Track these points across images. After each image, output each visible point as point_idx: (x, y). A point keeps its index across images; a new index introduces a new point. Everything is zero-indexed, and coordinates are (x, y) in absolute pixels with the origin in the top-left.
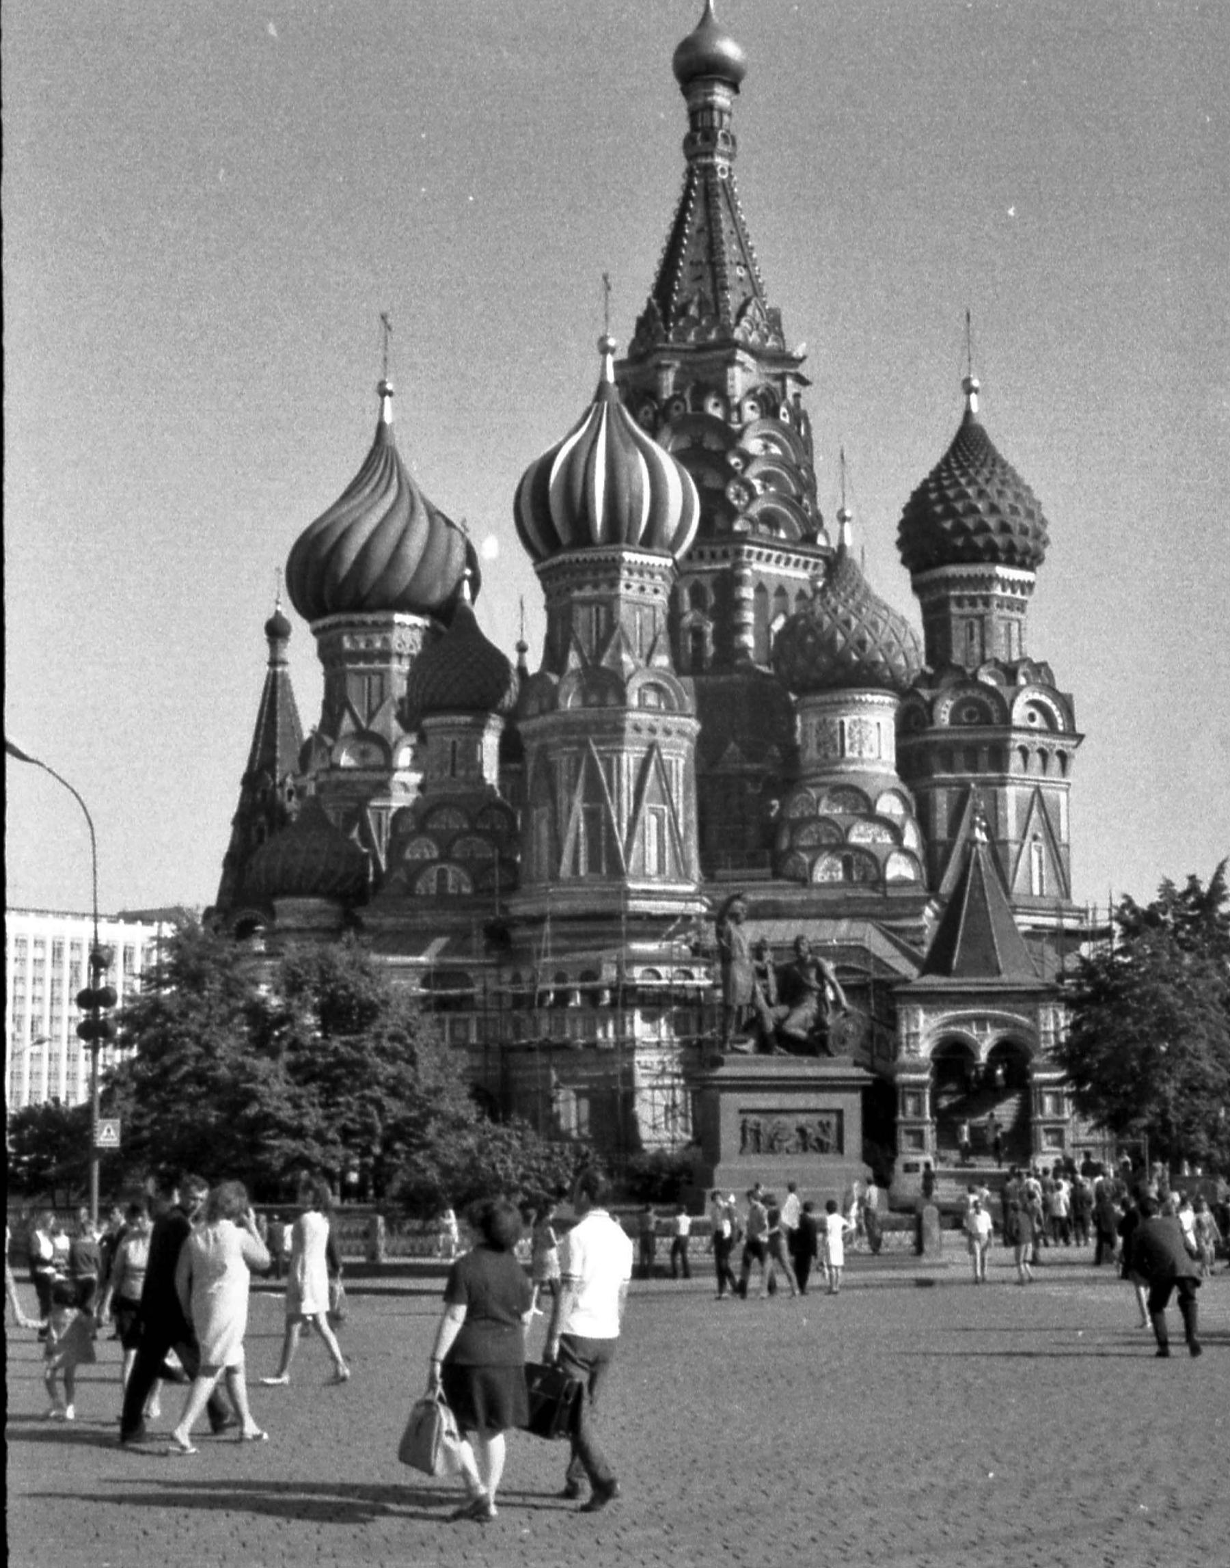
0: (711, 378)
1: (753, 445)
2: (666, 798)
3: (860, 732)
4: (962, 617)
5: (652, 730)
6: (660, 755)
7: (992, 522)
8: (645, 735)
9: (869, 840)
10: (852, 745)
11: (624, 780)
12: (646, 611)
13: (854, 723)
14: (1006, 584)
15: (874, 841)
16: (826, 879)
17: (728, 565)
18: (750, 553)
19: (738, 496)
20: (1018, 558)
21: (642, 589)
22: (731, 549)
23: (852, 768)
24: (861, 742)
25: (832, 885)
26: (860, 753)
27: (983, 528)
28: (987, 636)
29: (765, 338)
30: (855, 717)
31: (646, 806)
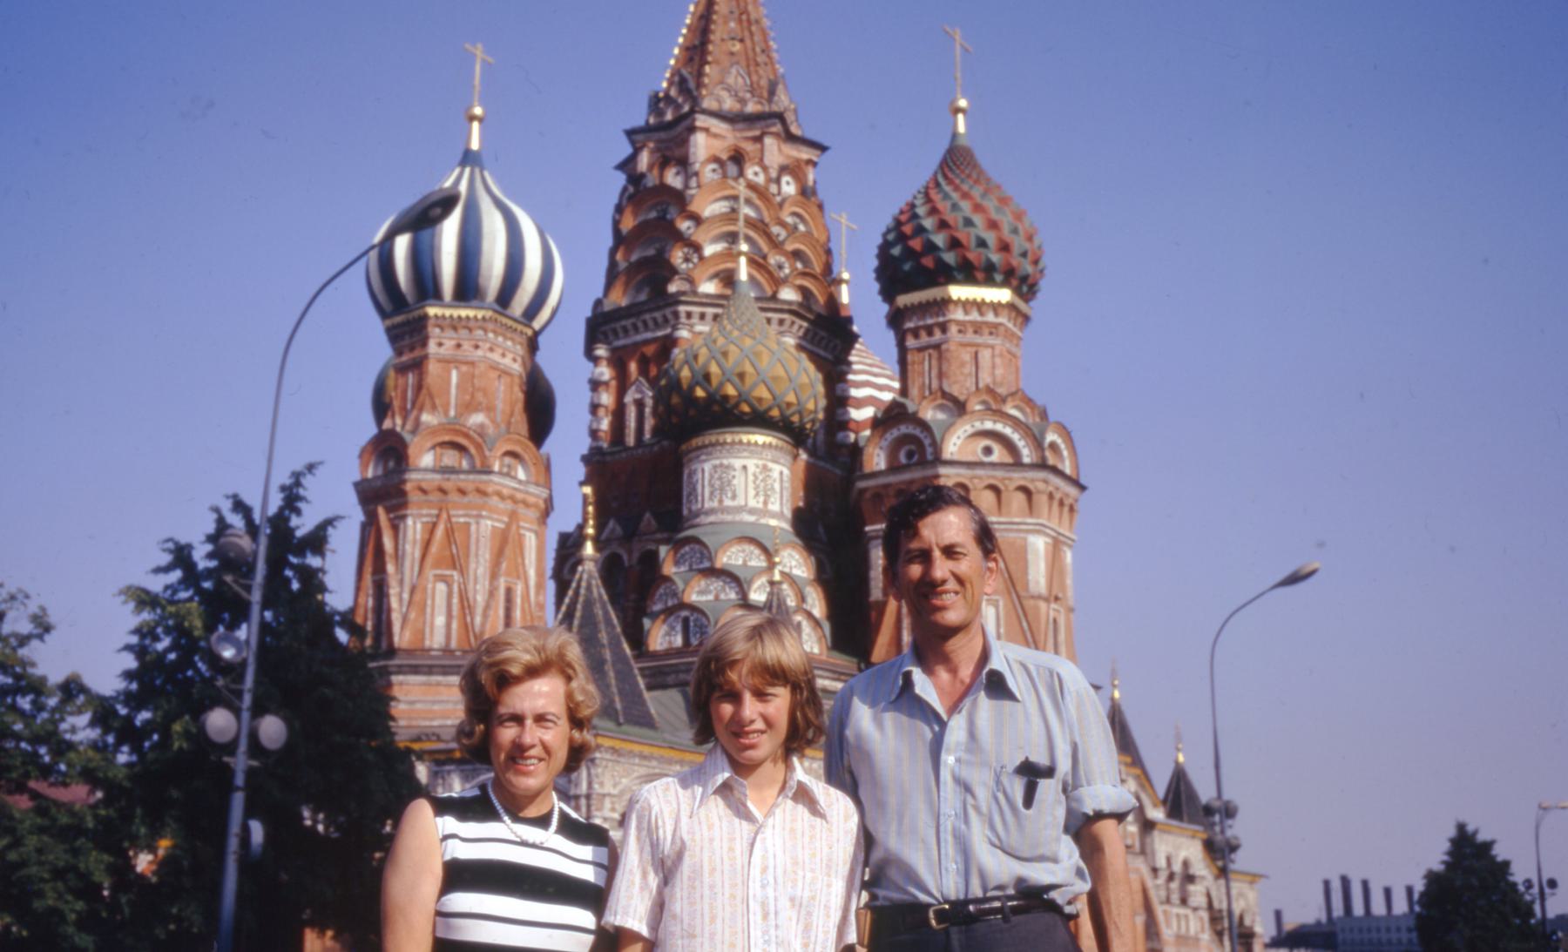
0: (678, 153)
1: (711, 208)
2: (456, 561)
3: (720, 478)
4: (921, 350)
5: (443, 491)
6: (449, 517)
7: (939, 239)
8: (435, 497)
9: (711, 597)
10: (712, 493)
11: (408, 548)
12: (464, 368)
13: (715, 467)
14: (967, 305)
15: (717, 598)
16: (665, 646)
17: (668, 331)
18: (689, 315)
19: (687, 260)
20: (980, 275)
21: (459, 346)
22: (668, 312)
23: (712, 518)
24: (722, 489)
25: (670, 653)
26: (721, 501)
27: (931, 247)
28: (944, 368)
29: (743, 101)
30: (717, 462)
31: (430, 573)
